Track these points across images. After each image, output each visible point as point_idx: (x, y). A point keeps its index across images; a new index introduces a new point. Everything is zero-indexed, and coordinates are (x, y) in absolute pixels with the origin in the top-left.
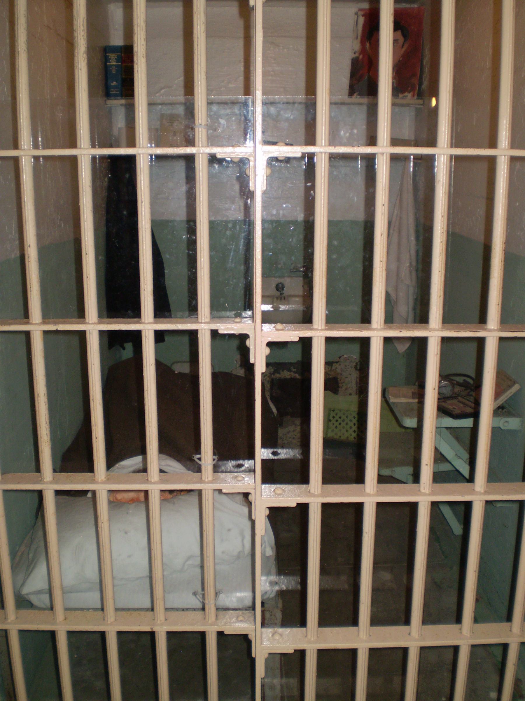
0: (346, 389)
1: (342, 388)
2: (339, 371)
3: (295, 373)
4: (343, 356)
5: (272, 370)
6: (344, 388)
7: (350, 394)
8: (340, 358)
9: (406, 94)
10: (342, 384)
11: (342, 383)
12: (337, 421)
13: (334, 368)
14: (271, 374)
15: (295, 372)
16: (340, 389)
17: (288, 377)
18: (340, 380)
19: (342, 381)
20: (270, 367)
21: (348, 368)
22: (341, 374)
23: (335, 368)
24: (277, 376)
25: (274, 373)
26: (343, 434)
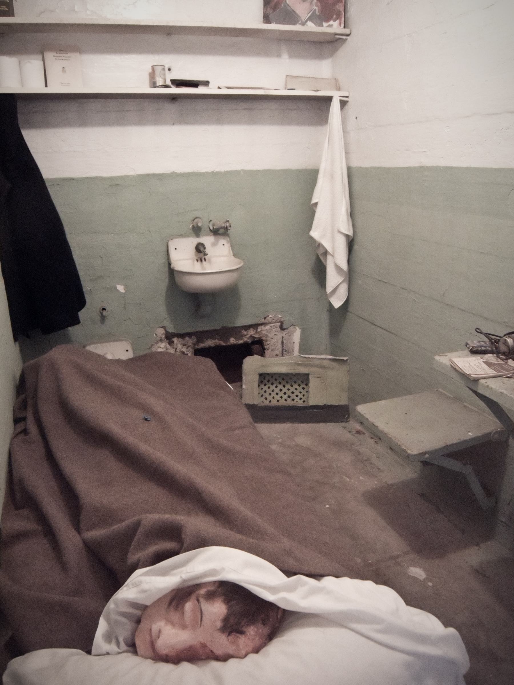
0: (273, 350)
1: (268, 349)
2: (264, 332)
3: (220, 340)
4: (268, 316)
5: (195, 340)
6: (270, 350)
7: (277, 355)
8: (265, 318)
9: (331, 22)
10: (268, 346)
11: (268, 345)
12: (293, 393)
13: (259, 330)
14: (194, 344)
15: (220, 340)
16: (266, 352)
17: (213, 345)
18: (266, 342)
19: (268, 343)
20: (193, 337)
21: (273, 329)
22: (267, 336)
23: (260, 330)
24: (202, 345)
25: (197, 343)
26: (273, 398)
